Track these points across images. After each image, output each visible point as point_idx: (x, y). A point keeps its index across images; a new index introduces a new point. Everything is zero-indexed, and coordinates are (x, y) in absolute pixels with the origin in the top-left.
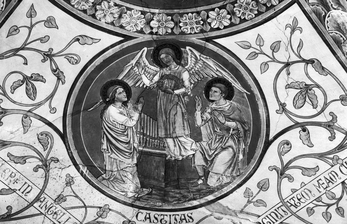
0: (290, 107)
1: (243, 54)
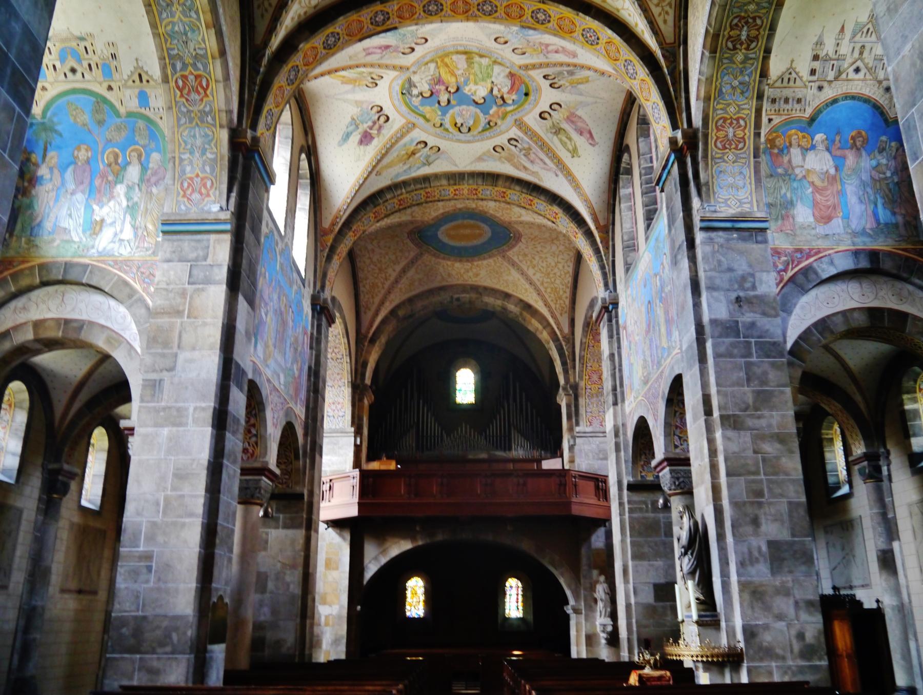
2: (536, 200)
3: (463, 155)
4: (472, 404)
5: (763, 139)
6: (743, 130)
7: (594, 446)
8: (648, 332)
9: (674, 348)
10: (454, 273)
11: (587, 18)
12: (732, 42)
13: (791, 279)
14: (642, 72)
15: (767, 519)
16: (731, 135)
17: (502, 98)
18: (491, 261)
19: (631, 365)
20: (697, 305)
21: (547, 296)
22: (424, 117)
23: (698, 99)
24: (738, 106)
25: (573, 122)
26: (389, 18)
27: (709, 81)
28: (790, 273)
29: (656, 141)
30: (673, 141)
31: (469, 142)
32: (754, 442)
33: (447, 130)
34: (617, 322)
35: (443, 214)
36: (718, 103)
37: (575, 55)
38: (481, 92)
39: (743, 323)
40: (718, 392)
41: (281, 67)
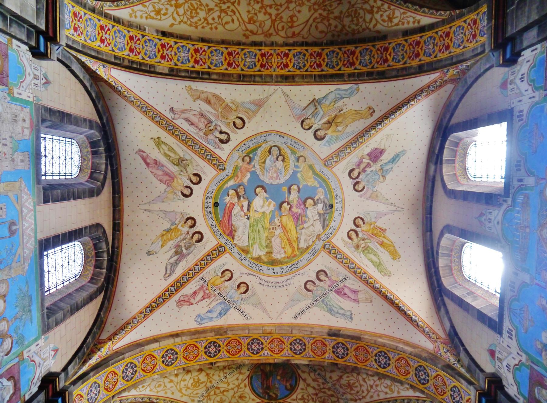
22: (314, 172)
31: (271, 133)
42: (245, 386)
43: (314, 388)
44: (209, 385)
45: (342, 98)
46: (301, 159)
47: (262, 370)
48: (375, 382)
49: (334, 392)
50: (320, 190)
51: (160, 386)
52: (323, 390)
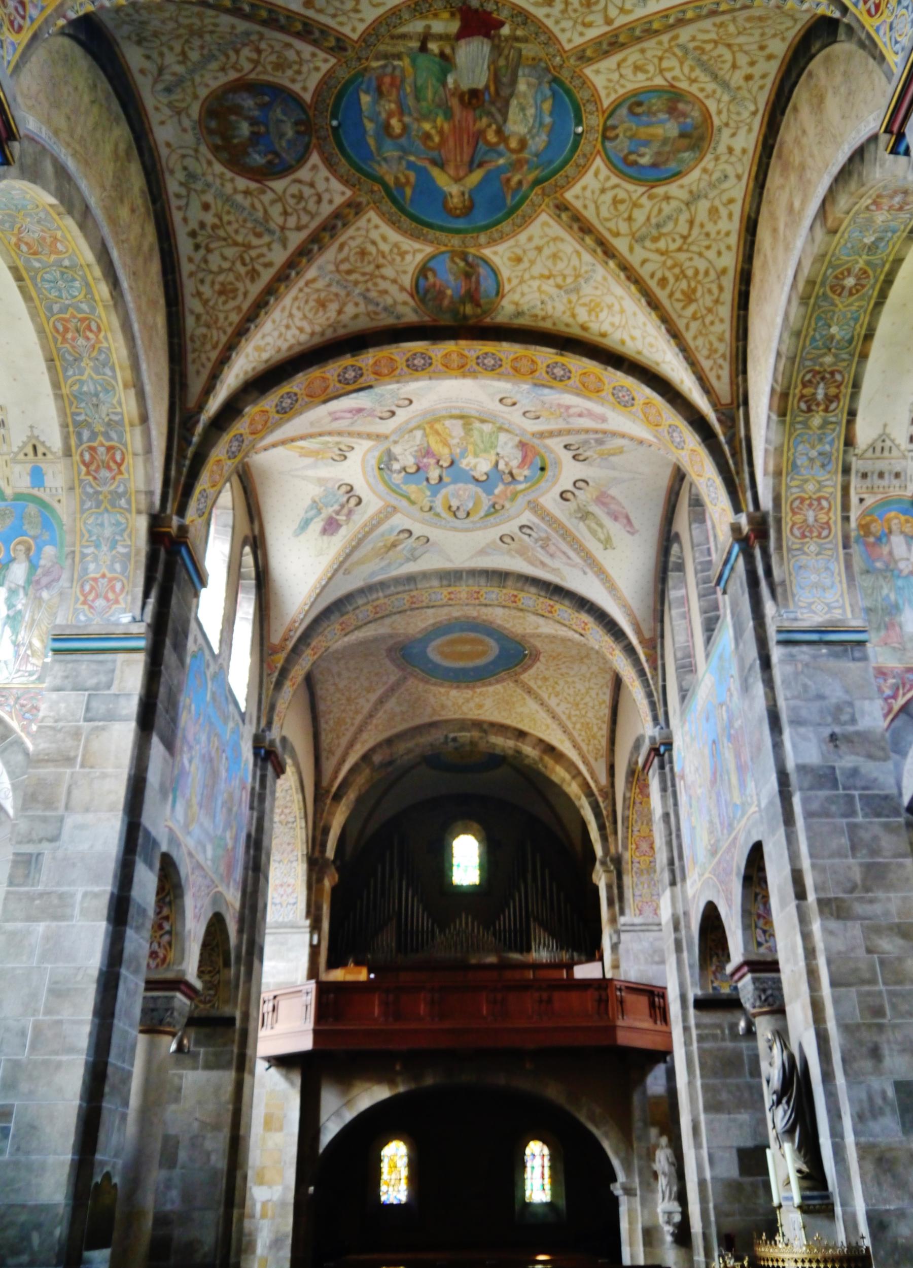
0: (649, 75)
1: (613, 97)
2: (558, 606)
3: (461, 547)
4: (475, 886)
5: (853, 524)
6: (827, 513)
7: (646, 944)
8: (714, 782)
9: (750, 805)
10: (449, 703)
11: (619, 374)
12: (806, 402)
13: (904, 709)
14: (692, 440)
15: (891, 1049)
16: (811, 520)
17: (511, 474)
18: (499, 687)
19: (693, 829)
20: (778, 746)
21: (575, 734)
22: (408, 499)
23: (766, 473)
24: (819, 482)
25: (604, 504)
26: (361, 375)
27: (779, 451)
28: (901, 701)
29: (714, 527)
30: (736, 529)
31: (467, 530)
32: (866, 938)
33: (438, 515)
34: (672, 769)
35: (433, 625)
36: (792, 479)
37: (604, 420)
38: (483, 466)
39: (840, 768)
40: (813, 866)
41: (219, 437)
42: (509, 280)
43: (383, 278)
44: (574, 297)
45: (382, 569)
46: (427, 509)
47: (478, 305)
48: (286, 340)
49: (346, 281)
50: (398, 482)
51: (651, 346)
52: (368, 277)
